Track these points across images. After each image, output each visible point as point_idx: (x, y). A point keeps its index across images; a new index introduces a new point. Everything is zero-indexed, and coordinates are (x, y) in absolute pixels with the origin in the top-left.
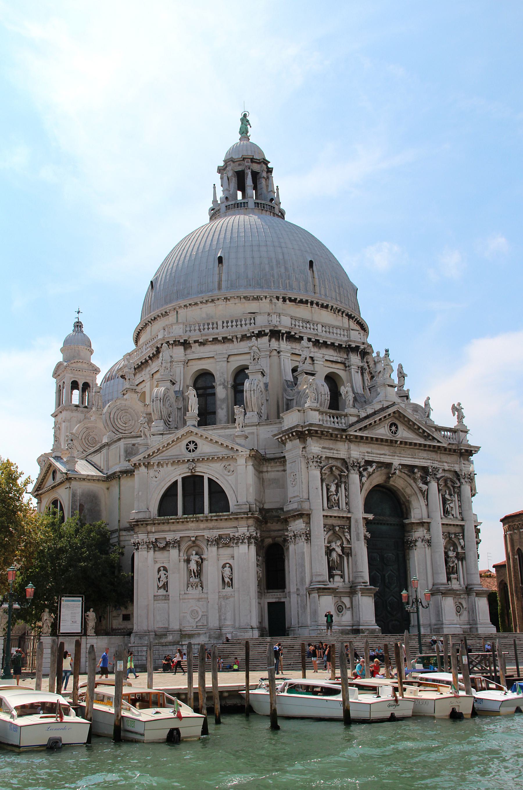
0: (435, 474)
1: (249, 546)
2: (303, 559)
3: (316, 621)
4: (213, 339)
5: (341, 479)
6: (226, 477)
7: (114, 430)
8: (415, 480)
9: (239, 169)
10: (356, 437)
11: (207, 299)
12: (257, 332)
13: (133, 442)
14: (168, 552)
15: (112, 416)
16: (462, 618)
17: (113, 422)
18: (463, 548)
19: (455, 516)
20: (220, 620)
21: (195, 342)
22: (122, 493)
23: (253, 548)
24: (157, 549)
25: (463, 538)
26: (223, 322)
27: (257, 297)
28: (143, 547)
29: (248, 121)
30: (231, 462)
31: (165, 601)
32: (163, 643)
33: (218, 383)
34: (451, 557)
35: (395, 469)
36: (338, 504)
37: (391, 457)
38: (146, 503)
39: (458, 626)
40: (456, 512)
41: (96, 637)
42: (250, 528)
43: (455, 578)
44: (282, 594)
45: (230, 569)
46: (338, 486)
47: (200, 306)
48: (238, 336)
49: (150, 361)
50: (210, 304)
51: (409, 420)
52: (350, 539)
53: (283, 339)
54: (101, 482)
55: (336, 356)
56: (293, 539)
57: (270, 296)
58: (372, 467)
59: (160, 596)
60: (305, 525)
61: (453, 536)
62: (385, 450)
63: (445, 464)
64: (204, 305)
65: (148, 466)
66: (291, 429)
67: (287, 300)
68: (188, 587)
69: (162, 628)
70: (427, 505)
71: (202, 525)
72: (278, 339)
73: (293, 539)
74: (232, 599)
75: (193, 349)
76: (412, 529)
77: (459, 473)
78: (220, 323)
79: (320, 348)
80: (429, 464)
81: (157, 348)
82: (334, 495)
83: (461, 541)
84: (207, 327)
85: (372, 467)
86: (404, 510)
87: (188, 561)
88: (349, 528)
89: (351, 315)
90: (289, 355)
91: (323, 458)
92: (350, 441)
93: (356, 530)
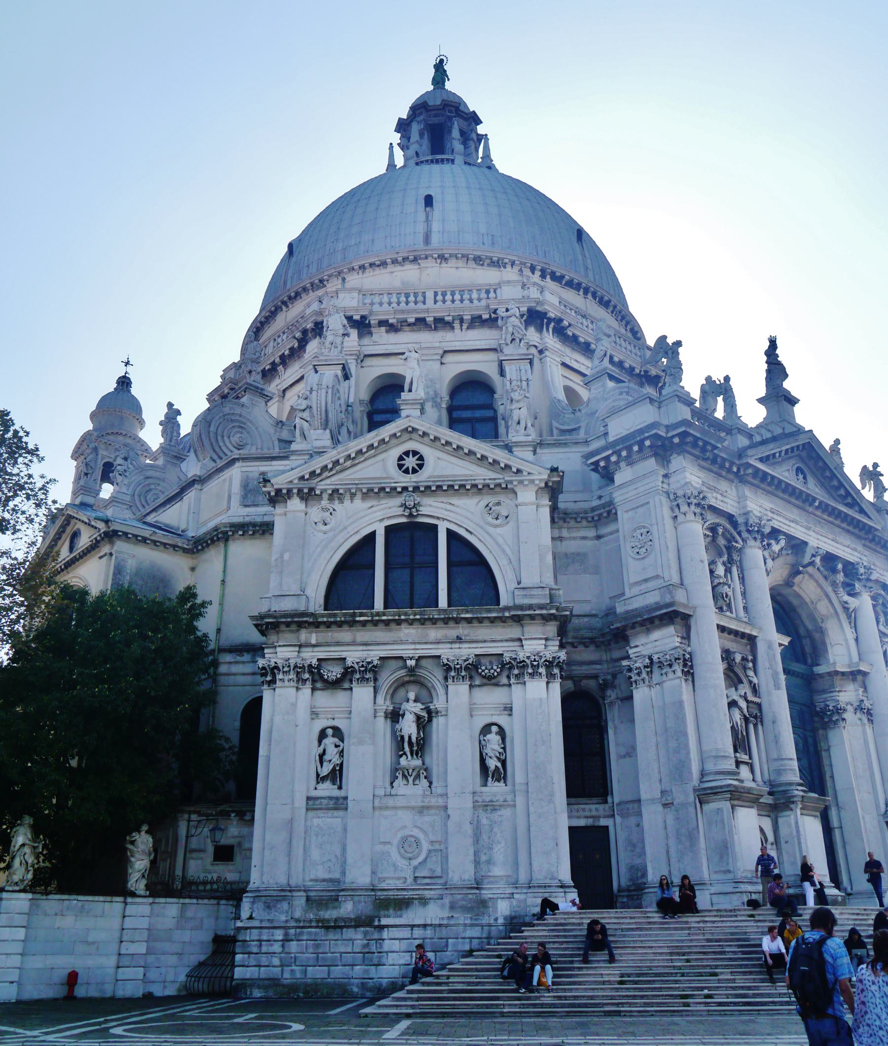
1: (548, 683)
2: (680, 718)
3: (729, 871)
4: (417, 320)
6: (491, 530)
7: (215, 457)
9: (435, 120)
10: (757, 470)
11: (406, 255)
13: (262, 469)
14: (349, 692)
15: (212, 429)
17: (213, 441)
20: (477, 863)
21: (382, 323)
22: (229, 572)
23: (556, 688)
24: (319, 685)
26: (436, 294)
27: (498, 261)
28: (286, 678)
29: (445, 71)
30: (502, 498)
31: (336, 813)
32: (328, 921)
35: (813, 556)
36: (729, 606)
37: (804, 530)
38: (298, 577)
41: (151, 900)
42: (550, 643)
44: (600, 807)
45: (498, 738)
47: (390, 268)
48: (465, 317)
49: (280, 368)
50: (408, 266)
53: (548, 330)
54: (181, 552)
56: (644, 675)
57: (521, 263)
58: (778, 542)
59: (321, 798)
60: (679, 640)
64: (399, 268)
65: (308, 496)
66: (641, 431)
67: (548, 277)
68: (393, 779)
69: (324, 880)
70: (857, 640)
71: (433, 633)
72: (540, 329)
73: (644, 675)
74: (506, 813)
75: (375, 337)
76: (833, 686)
78: (430, 295)
81: (305, 332)
84: (404, 299)
85: (778, 542)
86: (808, 649)
87: (395, 716)
88: (754, 661)
93: (771, 665)
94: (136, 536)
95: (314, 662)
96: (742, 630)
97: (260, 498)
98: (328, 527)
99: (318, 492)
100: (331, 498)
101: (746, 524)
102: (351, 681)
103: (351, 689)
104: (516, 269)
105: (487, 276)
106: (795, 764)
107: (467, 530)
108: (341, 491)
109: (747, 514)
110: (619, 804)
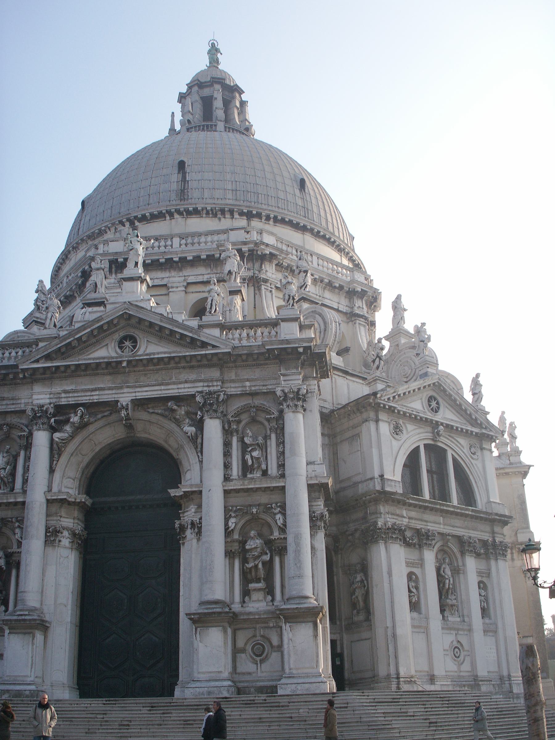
0: (211, 405)
8: (178, 423)
12: (80, 274)
16: (266, 666)
19: (269, 473)
29: (217, 50)
34: (251, 550)
37: (114, 392)
39: (230, 683)
43: (260, 590)
51: (151, 325)
52: (22, 538)
55: (208, 274)
62: (105, 382)
63: (248, 384)
79: (181, 270)
80: (200, 389)
89: (252, 212)
96: (5, 501)
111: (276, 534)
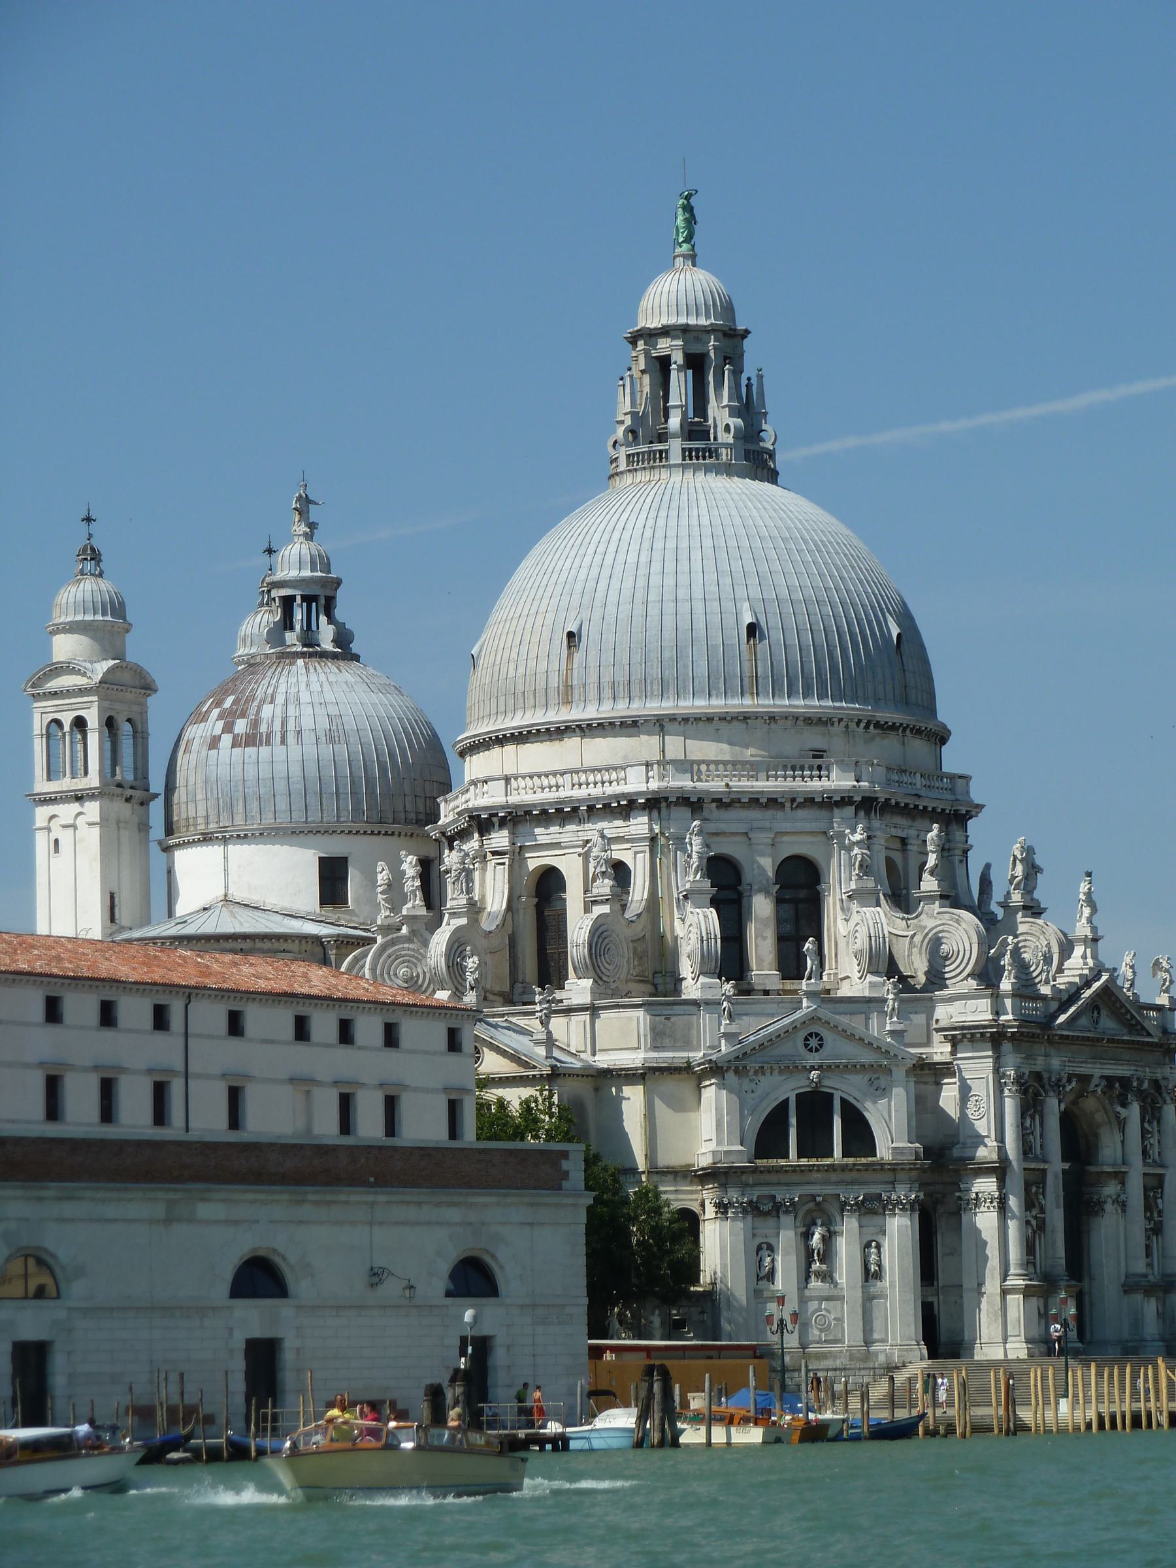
4: (750, 798)
5: (1035, 1106)
7: (597, 978)
9: (696, 349)
10: (1061, 1036)
14: (776, 1219)
18: (1160, 1213)
24: (755, 1213)
25: (1161, 1198)
33: (755, 887)
35: (1096, 1086)
40: (1154, 1153)
46: (1033, 1118)
50: (735, 723)
51: (1118, 999)
53: (876, 812)
58: (1069, 1081)
61: (1152, 1194)
63: (1147, 1070)
64: (724, 724)
70: (1123, 1142)
71: (834, 1177)
72: (868, 813)
75: (705, 813)
77: (1163, 1083)
79: (914, 820)
80: (1132, 1072)
82: (1030, 1133)
83: (1159, 1201)
87: (807, 1236)
88: (1044, 1188)
90: (883, 842)
91: (1026, 1077)
92: (1050, 1042)
94: (569, 1075)
95: (755, 1199)
97: (667, 1040)
98: (753, 1095)
99: (748, 1068)
100: (756, 1073)
101: (1050, 1079)
102: (778, 1212)
103: (779, 1217)
104: (843, 724)
105: (813, 738)
106: (1063, 1262)
107: (855, 1098)
108: (766, 1068)
109: (1050, 1071)
110: (943, 1287)
111: (1155, 1215)
